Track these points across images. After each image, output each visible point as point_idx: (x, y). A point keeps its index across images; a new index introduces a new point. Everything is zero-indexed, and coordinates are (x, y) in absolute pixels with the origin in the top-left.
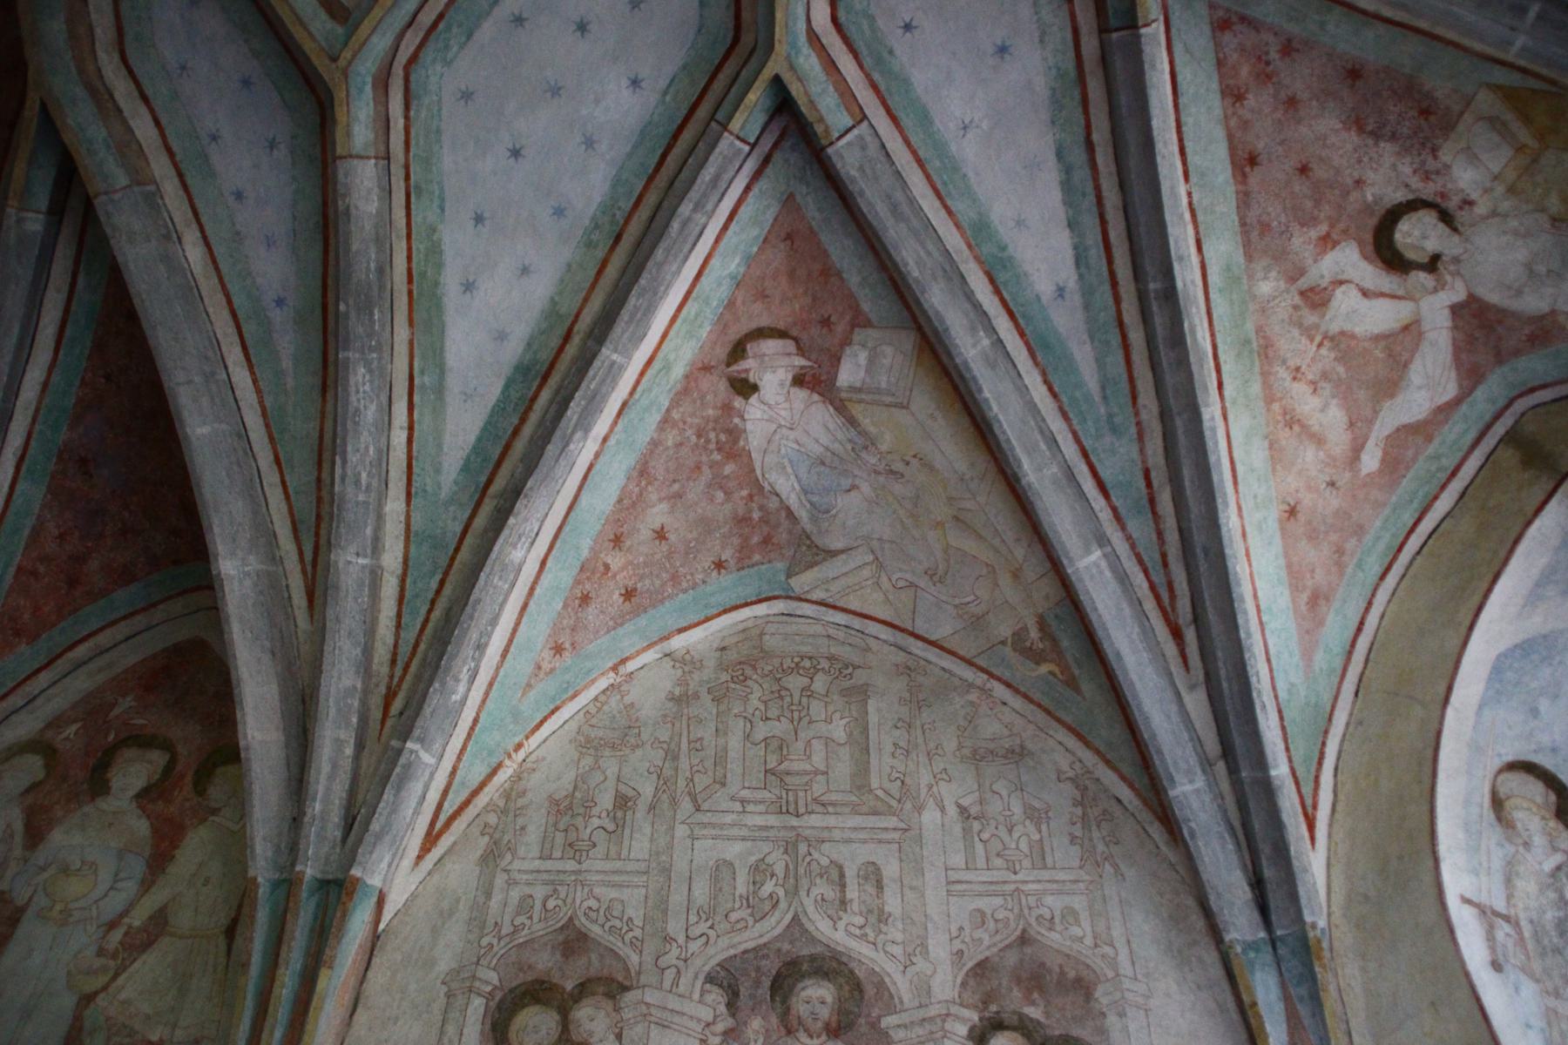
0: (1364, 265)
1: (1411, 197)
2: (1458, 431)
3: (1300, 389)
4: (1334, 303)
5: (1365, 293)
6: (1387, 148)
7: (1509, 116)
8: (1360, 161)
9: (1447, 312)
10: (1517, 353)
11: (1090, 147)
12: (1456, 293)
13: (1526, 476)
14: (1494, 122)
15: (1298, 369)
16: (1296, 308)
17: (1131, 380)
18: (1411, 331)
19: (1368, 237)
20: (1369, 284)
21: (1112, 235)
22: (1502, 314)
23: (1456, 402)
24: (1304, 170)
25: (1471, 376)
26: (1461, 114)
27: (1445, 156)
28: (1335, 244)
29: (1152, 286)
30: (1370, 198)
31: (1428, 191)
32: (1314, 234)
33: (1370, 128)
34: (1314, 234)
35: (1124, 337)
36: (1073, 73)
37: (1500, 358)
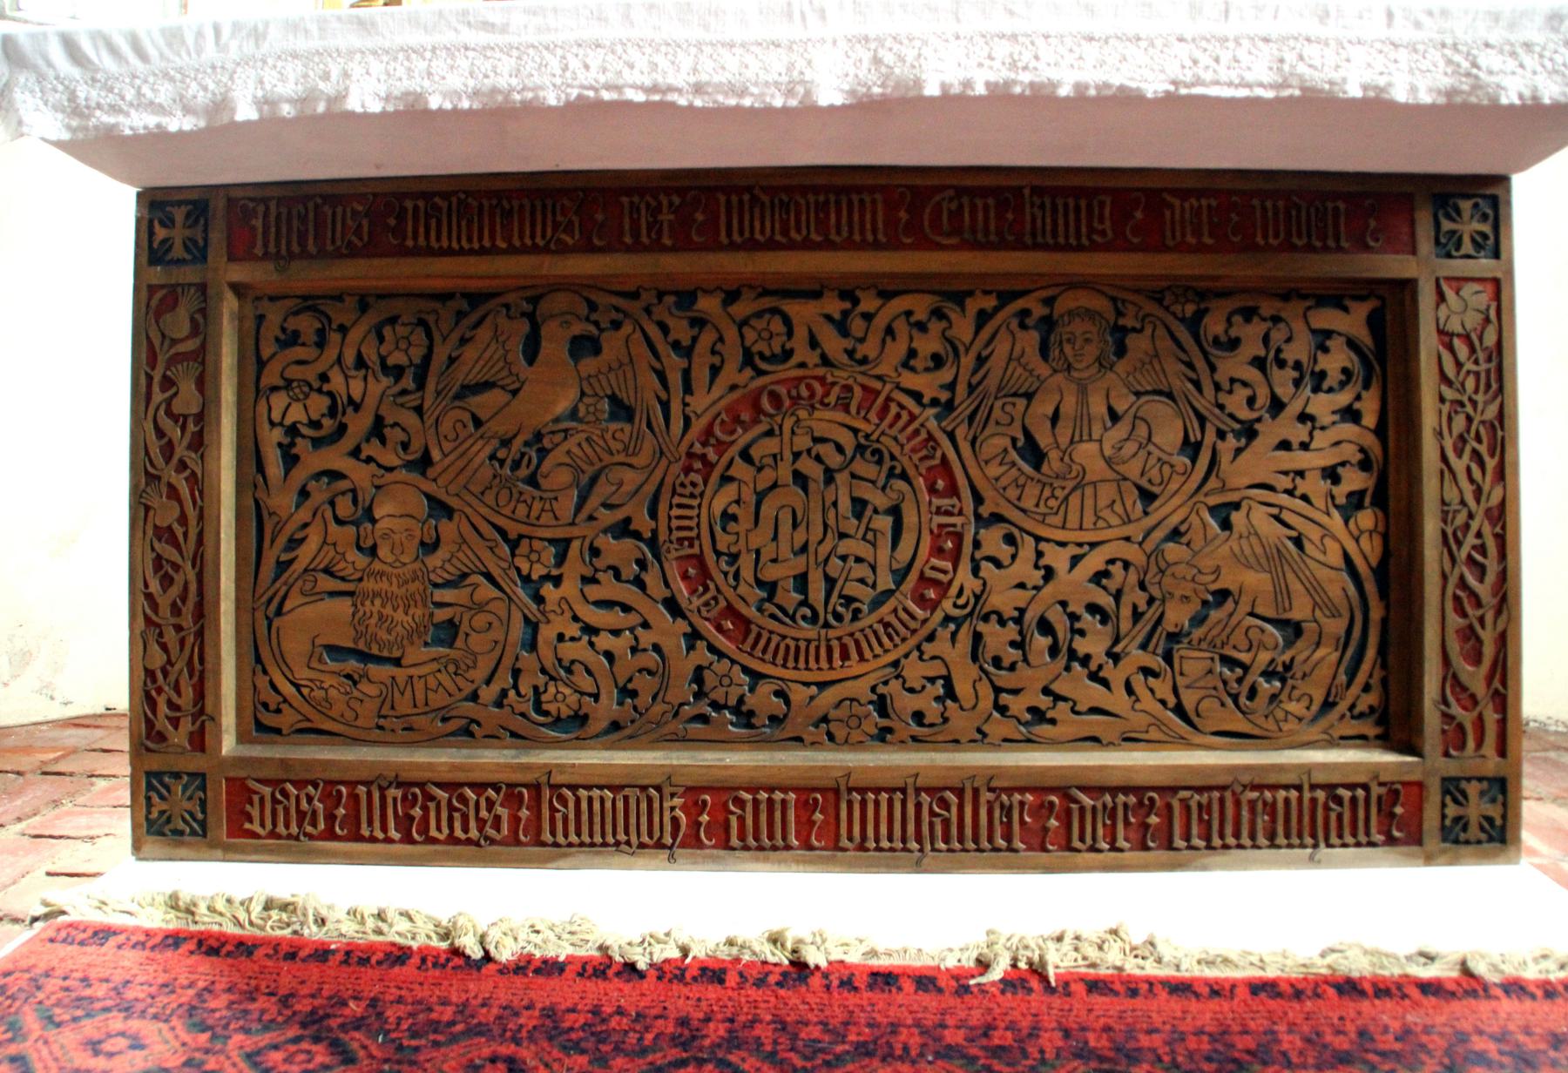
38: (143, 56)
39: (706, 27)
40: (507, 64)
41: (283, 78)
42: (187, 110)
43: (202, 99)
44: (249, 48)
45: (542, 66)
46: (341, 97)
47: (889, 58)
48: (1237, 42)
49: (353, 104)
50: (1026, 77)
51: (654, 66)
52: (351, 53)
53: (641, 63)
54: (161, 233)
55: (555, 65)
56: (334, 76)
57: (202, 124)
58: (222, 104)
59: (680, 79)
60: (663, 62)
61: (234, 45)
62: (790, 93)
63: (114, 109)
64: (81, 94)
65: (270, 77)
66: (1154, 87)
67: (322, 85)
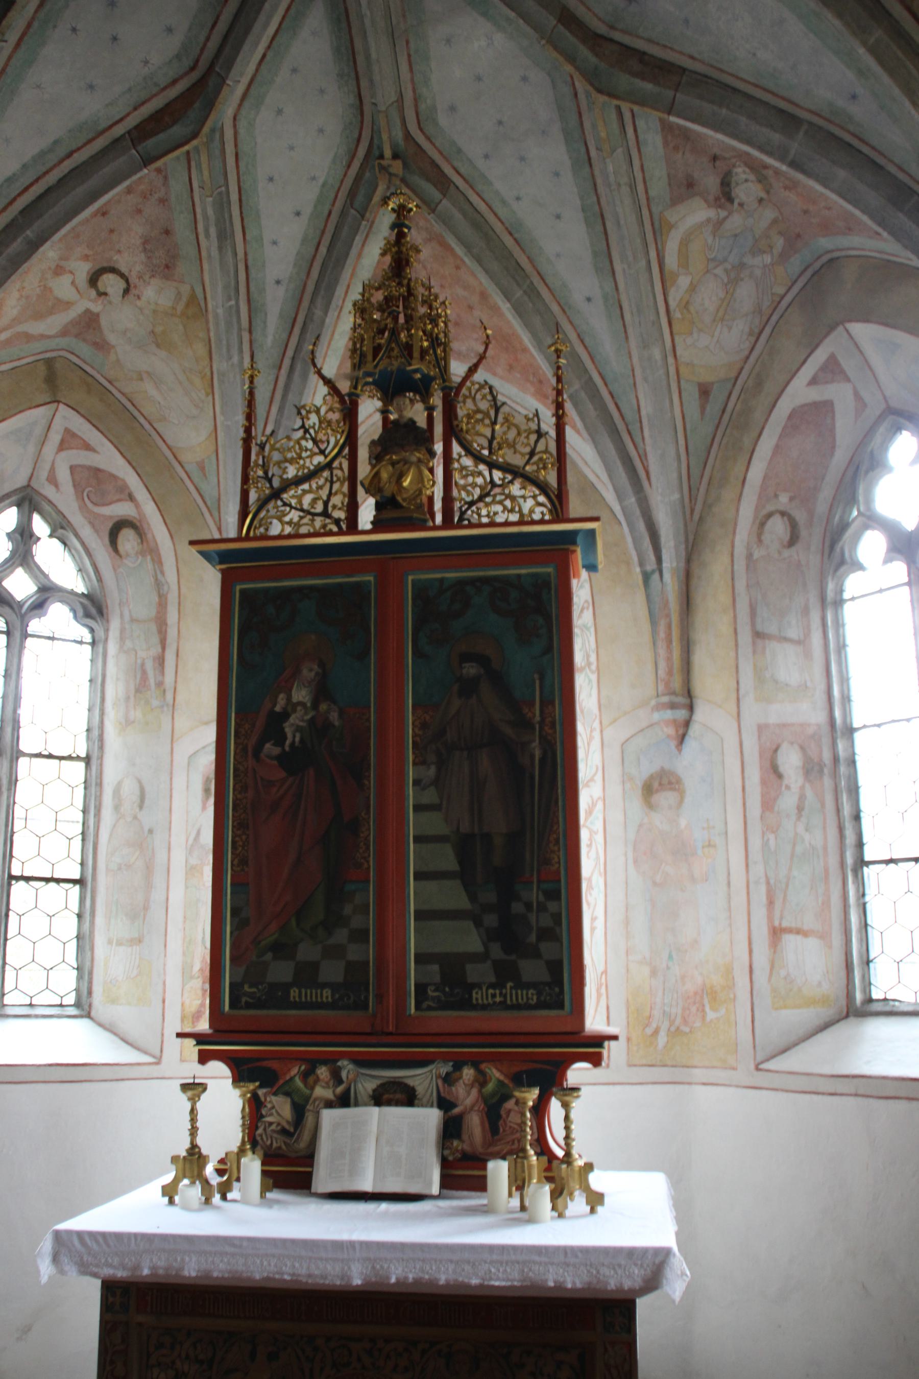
3: (16, 294)
6: (143, 257)
11: (70, 155)
20: (77, 281)
21: (34, 188)
24: (112, 231)
26: (175, 281)
27: (154, 281)
32: (87, 252)
33: (147, 247)
34: (87, 252)
36: (101, 128)
38: (108, 1246)
46: (182, 1269)
54: (111, 1299)
63: (97, 1266)
64: (85, 1259)
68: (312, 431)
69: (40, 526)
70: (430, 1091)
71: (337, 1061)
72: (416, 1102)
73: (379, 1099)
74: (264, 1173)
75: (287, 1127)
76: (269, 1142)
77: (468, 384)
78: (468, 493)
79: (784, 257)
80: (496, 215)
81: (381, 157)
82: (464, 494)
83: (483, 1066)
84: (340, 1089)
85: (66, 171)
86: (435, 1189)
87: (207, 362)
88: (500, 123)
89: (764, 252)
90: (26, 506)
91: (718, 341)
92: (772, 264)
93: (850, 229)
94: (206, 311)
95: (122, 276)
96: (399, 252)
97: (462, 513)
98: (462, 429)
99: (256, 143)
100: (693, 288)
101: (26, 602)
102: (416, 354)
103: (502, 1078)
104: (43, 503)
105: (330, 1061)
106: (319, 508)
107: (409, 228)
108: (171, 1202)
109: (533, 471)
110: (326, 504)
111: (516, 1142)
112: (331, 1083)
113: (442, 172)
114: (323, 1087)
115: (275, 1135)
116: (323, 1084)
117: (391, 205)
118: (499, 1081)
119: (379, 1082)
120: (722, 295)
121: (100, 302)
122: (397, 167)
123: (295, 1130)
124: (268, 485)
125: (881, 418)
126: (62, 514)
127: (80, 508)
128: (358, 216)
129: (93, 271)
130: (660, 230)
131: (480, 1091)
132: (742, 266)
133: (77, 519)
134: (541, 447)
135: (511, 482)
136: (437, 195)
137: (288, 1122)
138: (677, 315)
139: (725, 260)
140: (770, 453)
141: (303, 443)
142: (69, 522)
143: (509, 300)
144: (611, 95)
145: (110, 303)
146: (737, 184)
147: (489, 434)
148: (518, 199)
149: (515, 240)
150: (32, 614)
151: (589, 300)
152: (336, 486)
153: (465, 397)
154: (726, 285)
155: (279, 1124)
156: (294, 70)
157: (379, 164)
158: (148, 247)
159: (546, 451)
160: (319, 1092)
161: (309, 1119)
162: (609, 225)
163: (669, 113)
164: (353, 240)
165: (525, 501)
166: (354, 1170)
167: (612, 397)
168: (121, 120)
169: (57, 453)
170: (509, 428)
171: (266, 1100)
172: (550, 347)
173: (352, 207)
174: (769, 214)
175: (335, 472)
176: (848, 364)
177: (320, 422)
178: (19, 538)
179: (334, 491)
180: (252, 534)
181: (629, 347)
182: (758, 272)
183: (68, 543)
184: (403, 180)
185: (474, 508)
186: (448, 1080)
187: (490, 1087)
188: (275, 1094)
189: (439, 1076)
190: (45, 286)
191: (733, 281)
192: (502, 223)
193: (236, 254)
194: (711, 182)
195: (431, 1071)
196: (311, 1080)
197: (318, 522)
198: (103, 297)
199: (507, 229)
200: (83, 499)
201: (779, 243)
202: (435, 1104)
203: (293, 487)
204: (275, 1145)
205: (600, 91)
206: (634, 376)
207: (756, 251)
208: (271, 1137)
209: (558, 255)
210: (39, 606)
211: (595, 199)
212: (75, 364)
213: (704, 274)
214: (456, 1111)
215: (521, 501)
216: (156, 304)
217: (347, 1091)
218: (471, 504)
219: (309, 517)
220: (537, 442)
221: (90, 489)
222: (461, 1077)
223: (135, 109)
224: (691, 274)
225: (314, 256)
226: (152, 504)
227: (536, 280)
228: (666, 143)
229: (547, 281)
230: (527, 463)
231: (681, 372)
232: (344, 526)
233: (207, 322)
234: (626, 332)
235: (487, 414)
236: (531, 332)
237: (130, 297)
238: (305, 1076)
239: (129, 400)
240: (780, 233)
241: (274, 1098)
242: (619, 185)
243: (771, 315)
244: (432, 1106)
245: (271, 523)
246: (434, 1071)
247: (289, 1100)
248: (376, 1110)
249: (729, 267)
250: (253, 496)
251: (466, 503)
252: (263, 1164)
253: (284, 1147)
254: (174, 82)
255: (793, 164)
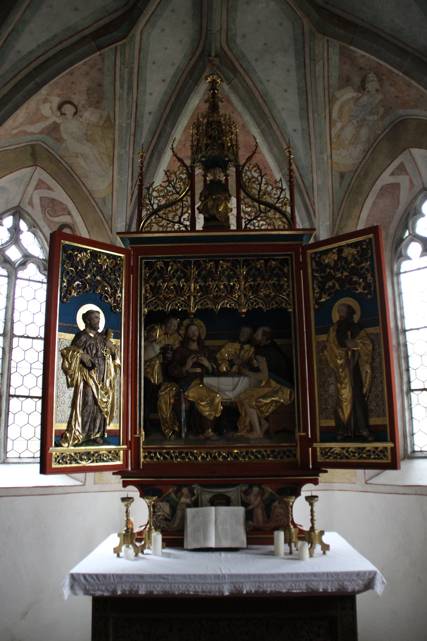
0: (57, 103)
1: (77, 105)
2: (29, 138)
4: (46, 104)
5: (51, 108)
6: (86, 97)
7: (104, 119)
8: (80, 92)
9: (53, 121)
10: (51, 137)
11: (61, 43)
12: (58, 121)
13: (30, 158)
14: (101, 116)
15: (28, 108)
16: (42, 99)
17: (8, 82)
18: (47, 118)
19: (63, 101)
21: (41, 58)
22: (59, 131)
23: (35, 134)
25: (42, 132)
27: (90, 109)
28: (59, 97)
29: (37, 79)
30: (72, 97)
31: (80, 108)
33: (89, 92)
35: (18, 74)
37: (48, 134)
39: (204, 580)
40: (168, 586)
41: (126, 586)
42: (108, 591)
43: (111, 590)
44: (119, 580)
45: (175, 587)
47: (237, 586)
48: (300, 582)
49: (140, 593)
50: (261, 590)
51: (195, 587)
52: (139, 582)
53: (192, 586)
55: (177, 586)
56: (136, 586)
57: (111, 594)
58: (115, 591)
59: (200, 590)
60: (197, 587)
61: (117, 579)
62: (219, 593)
65: (124, 586)
66: (284, 591)
67: (134, 589)
68: (172, 183)
69: (23, 225)
70: (238, 497)
71: (192, 485)
72: (231, 503)
73: (213, 502)
74: (163, 540)
75: (167, 516)
76: (159, 524)
77: (248, 165)
78: (249, 215)
79: (383, 117)
80: (256, 88)
81: (210, 55)
82: (247, 216)
83: (263, 486)
84: (193, 499)
85: (59, 50)
86: (245, 545)
87: (112, 149)
88: (266, 44)
89: (375, 114)
90: (18, 216)
91: (350, 154)
92: (377, 120)
93: (416, 106)
94: (114, 125)
95: (74, 106)
96: (214, 101)
97: (246, 225)
98: (246, 185)
99: (150, 44)
100: (342, 128)
101: (17, 262)
102: (226, 149)
103: (272, 491)
104: (25, 214)
105: (189, 485)
106: (177, 219)
107: (218, 90)
108: (118, 556)
109: (280, 206)
110: (180, 218)
111: (279, 522)
112: (189, 496)
113: (234, 65)
114: (185, 498)
115: (162, 521)
116: (185, 496)
117: (209, 80)
118: (271, 493)
119: (212, 495)
120: (354, 132)
121: (61, 118)
122: (216, 61)
123: (172, 517)
124: (151, 208)
125: (420, 192)
126: (34, 220)
127: (44, 218)
128: (194, 83)
129: (61, 102)
130: (331, 100)
131: (261, 498)
132: (364, 120)
133: (41, 223)
134: (282, 196)
135: (269, 211)
136: (232, 76)
137: (168, 515)
138: (334, 140)
139: (358, 117)
140: (371, 206)
141: (168, 188)
142: (37, 224)
143: (259, 128)
144: (324, 34)
145: (66, 119)
146: (368, 82)
147: (258, 189)
148: (268, 81)
149: (264, 100)
150: (20, 268)
151: (295, 130)
152: (185, 210)
153: (247, 171)
154: (357, 128)
155: (163, 516)
156: (173, 11)
157: (208, 59)
158: (89, 92)
159: (285, 198)
160: (183, 500)
161: (179, 513)
162: (309, 96)
163: (351, 45)
164: (190, 94)
165: (276, 220)
166: (206, 537)
167: (301, 176)
168: (88, 27)
169: (34, 191)
170: (268, 186)
171: (157, 504)
172: (286, 149)
173: (191, 79)
174: (380, 97)
175: (184, 203)
176: (409, 167)
177: (177, 179)
178: (14, 231)
179: (184, 211)
180: (144, 231)
181: (311, 154)
182: (371, 123)
183: (36, 234)
184: (218, 68)
185: (252, 222)
186: (247, 493)
187: (267, 495)
188: (162, 501)
189: (241, 491)
190: (38, 108)
191: (360, 126)
192: (259, 92)
193: (133, 98)
194: (357, 80)
195: (238, 489)
196: (179, 494)
197: (176, 226)
198: (63, 115)
199: (261, 95)
200: (45, 214)
201: (382, 111)
202: (240, 504)
203: (164, 209)
204: (162, 526)
205: (319, 32)
206: (312, 167)
207: (371, 113)
208: (160, 522)
209: (283, 109)
210: (23, 264)
211: (304, 83)
212: (44, 148)
213: (348, 122)
214: (250, 507)
215: (274, 220)
216: (90, 120)
217: (197, 499)
218: (250, 221)
219: (172, 223)
220: (281, 193)
221: (49, 209)
222: (252, 492)
223: (96, 22)
224: (342, 122)
225: (168, 102)
226: (80, 217)
227: (271, 120)
228: (340, 60)
229: (276, 121)
230: (276, 203)
231: (333, 167)
232: (189, 229)
233: (114, 130)
234: (310, 146)
235: (257, 179)
236: (268, 143)
237: (77, 116)
238: (176, 493)
239: (70, 167)
240: (383, 106)
241: (161, 503)
242: (319, 77)
243: (374, 143)
244: (238, 506)
245: (153, 226)
246: (239, 489)
247: (168, 504)
248: (213, 508)
249: (358, 119)
250: (144, 213)
251: (248, 220)
252: (163, 536)
253: (166, 526)
254: (116, 10)
255: (404, 73)
